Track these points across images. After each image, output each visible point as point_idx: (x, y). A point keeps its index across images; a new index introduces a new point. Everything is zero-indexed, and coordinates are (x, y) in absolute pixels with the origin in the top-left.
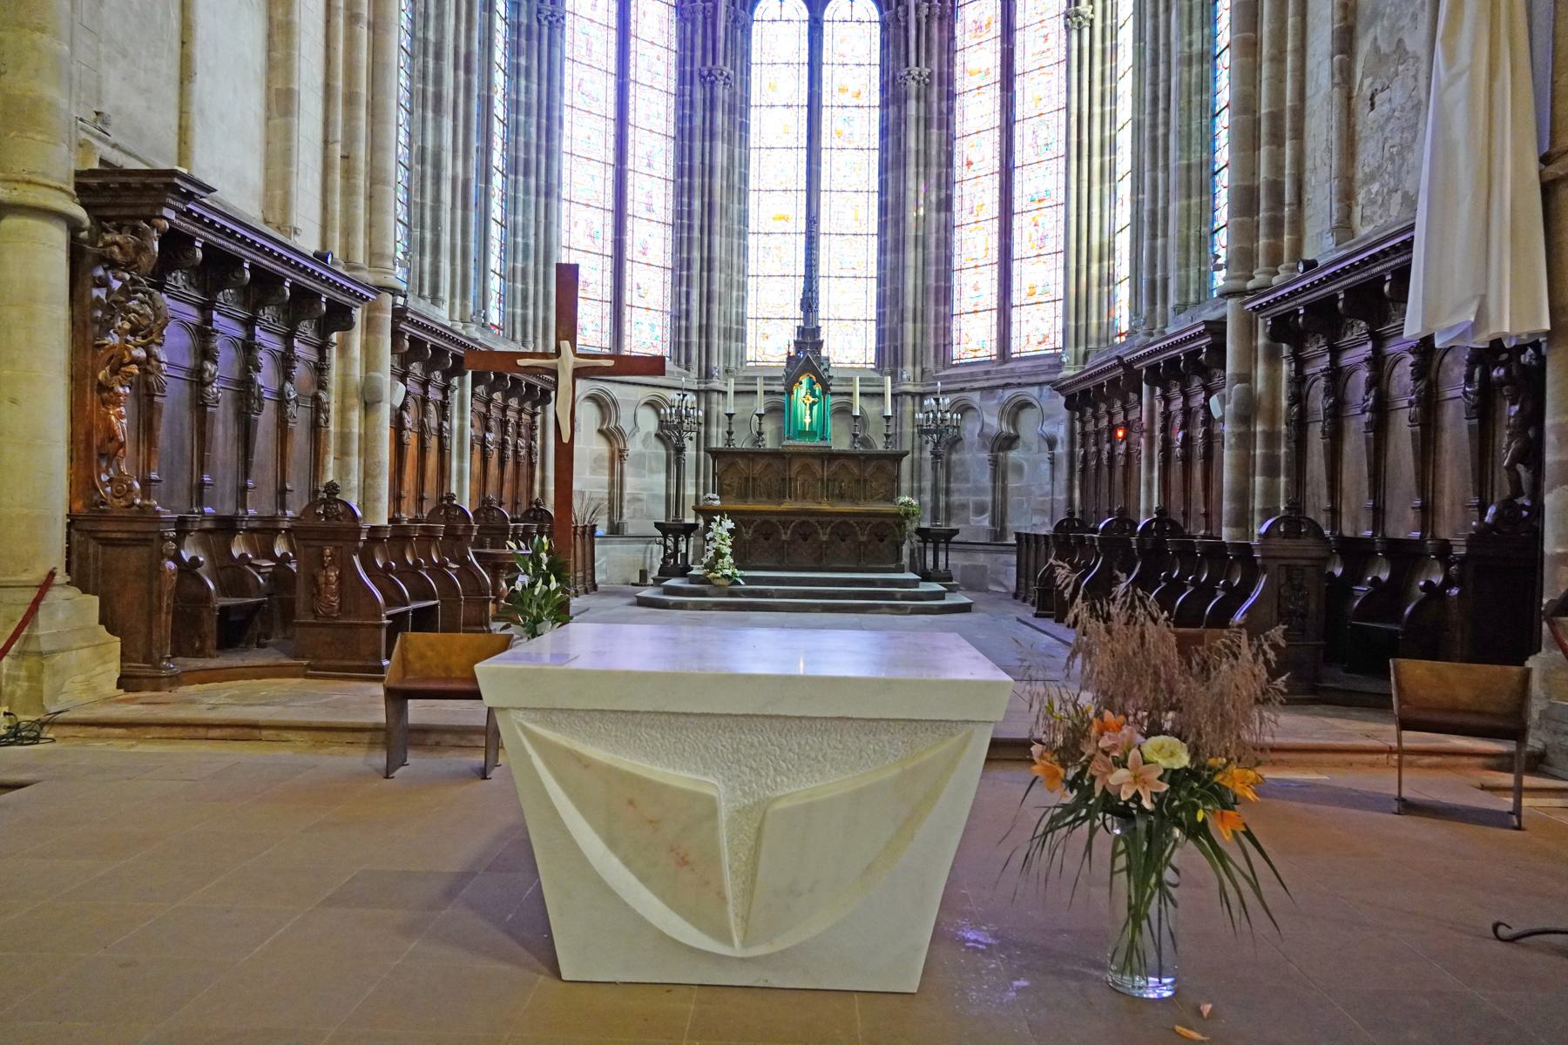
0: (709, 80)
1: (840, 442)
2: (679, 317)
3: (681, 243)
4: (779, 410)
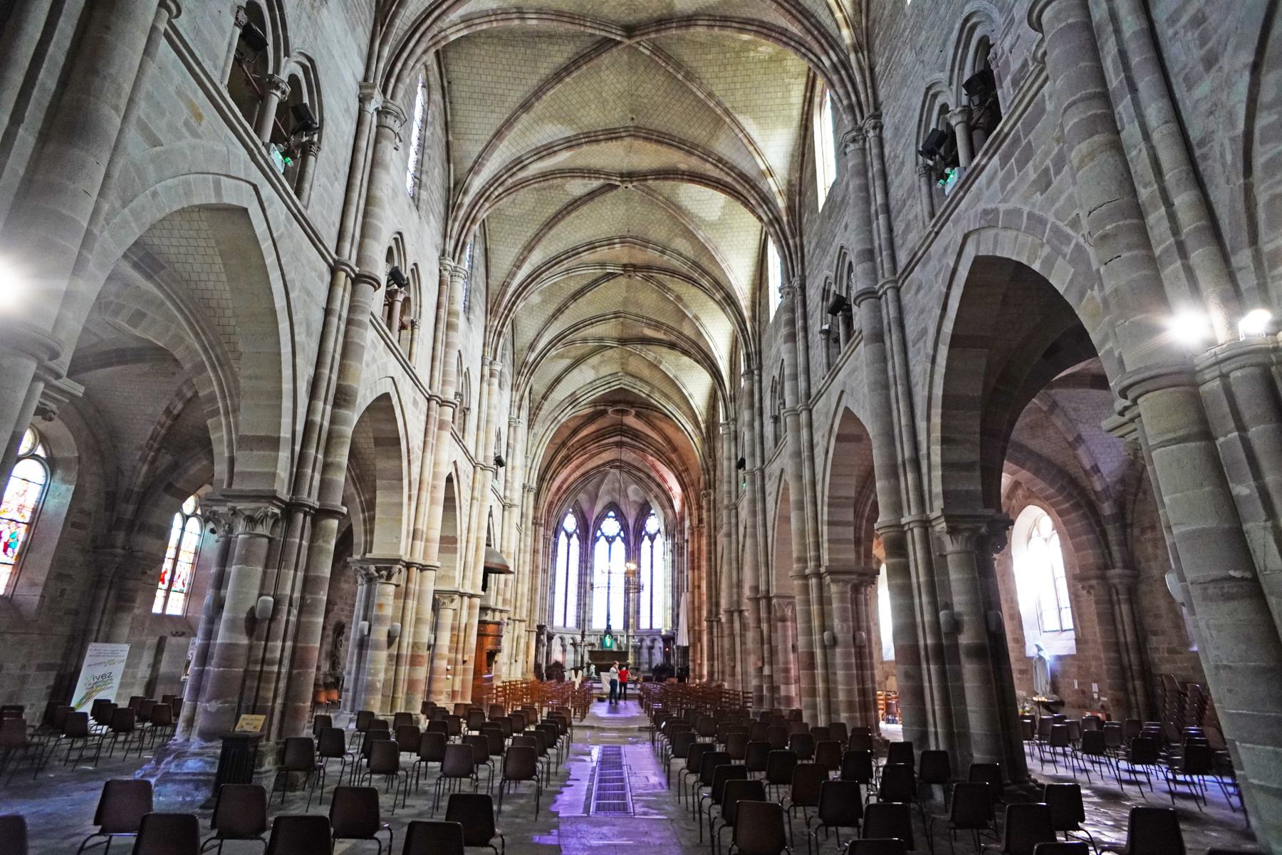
0: (586, 562)
1: (615, 649)
2: (578, 617)
3: (579, 599)
4: (602, 640)
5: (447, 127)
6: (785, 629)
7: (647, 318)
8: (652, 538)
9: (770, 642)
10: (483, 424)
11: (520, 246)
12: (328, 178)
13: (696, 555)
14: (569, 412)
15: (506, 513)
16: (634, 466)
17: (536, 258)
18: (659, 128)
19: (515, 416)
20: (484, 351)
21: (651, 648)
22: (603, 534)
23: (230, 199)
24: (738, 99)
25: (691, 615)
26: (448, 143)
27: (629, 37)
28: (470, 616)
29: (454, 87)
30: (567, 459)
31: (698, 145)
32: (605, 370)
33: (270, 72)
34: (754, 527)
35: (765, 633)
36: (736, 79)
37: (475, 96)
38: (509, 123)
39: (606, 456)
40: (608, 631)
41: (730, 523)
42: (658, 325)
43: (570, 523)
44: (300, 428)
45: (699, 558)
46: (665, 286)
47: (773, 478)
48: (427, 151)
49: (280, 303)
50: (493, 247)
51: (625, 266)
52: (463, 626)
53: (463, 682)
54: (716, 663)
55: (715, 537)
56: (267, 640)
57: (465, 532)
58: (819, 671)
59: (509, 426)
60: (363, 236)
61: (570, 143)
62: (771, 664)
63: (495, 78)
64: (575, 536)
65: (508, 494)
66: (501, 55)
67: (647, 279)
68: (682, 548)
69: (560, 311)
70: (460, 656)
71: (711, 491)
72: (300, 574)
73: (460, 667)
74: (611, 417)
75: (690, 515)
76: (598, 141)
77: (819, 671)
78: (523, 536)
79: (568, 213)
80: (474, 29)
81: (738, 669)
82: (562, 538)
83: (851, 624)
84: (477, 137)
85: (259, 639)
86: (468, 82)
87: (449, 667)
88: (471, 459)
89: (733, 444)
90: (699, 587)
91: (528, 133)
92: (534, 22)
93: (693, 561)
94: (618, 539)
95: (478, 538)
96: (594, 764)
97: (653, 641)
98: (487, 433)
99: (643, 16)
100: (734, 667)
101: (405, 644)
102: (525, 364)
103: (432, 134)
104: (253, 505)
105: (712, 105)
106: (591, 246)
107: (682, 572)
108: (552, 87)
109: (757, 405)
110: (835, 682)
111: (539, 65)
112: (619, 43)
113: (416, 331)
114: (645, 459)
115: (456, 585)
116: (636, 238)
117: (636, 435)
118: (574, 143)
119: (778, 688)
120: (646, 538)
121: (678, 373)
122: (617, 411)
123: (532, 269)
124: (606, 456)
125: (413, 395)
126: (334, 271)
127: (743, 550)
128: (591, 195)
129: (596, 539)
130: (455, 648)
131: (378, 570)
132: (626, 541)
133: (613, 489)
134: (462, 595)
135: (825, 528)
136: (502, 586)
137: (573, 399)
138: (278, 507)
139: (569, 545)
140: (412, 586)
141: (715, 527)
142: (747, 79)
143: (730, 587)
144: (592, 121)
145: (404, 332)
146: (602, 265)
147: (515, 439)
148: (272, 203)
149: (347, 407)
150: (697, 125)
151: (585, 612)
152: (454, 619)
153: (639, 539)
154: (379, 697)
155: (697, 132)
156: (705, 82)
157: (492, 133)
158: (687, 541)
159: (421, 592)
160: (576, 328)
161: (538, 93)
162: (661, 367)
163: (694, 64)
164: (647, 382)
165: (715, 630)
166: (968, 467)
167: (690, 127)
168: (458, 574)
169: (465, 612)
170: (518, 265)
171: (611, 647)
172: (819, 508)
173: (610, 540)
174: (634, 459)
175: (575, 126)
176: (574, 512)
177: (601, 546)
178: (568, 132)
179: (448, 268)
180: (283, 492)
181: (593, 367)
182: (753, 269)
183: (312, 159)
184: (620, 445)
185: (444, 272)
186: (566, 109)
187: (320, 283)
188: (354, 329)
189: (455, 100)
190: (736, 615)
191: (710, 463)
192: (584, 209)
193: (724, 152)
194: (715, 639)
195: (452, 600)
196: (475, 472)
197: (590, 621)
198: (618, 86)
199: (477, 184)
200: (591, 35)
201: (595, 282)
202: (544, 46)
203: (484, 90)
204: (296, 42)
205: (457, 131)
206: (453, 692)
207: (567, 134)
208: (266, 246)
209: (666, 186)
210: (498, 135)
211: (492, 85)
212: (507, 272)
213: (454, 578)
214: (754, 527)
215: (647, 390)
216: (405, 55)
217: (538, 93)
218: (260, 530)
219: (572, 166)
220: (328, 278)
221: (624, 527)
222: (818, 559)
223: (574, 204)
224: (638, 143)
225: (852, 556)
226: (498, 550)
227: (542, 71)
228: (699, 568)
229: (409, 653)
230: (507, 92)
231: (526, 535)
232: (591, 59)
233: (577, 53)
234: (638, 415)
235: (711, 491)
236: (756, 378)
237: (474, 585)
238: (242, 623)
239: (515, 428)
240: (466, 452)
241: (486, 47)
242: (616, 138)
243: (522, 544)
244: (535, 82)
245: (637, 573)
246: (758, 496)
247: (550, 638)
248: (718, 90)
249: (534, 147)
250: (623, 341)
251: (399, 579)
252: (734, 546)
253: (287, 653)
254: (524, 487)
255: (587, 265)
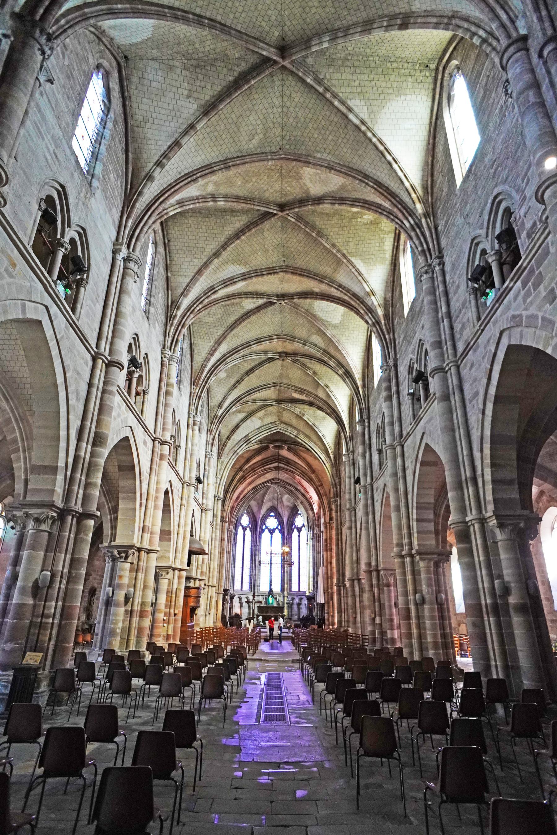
0: (256, 546)
1: (275, 605)
2: (250, 583)
3: (251, 572)
5: (167, 268)
6: (389, 592)
7: (295, 386)
8: (299, 530)
9: (379, 600)
10: (188, 456)
11: (212, 341)
12: (92, 301)
13: (328, 542)
14: (244, 448)
15: (203, 514)
16: (287, 483)
17: (223, 349)
18: (301, 267)
19: (209, 451)
20: (189, 409)
21: (299, 604)
22: (267, 528)
23: (30, 315)
24: (351, 247)
25: (325, 582)
26: (167, 278)
27: (282, 211)
28: (179, 583)
29: (172, 243)
30: (243, 478)
31: (326, 277)
32: (268, 420)
33: (58, 237)
34: (367, 523)
35: (376, 594)
36: (349, 235)
37: (185, 248)
38: (206, 265)
39: (269, 476)
40: (271, 593)
41: (351, 520)
42: (301, 391)
43: (245, 520)
44: (71, 460)
45: (330, 544)
46: (305, 366)
47: (379, 490)
48: (155, 283)
49: (60, 379)
50: (195, 342)
51: (280, 353)
52: (174, 590)
53: (174, 628)
54: (343, 614)
55: (341, 530)
56: (45, 602)
57: (176, 527)
58: (413, 621)
59: (206, 457)
60: (113, 336)
61: (245, 277)
62: (381, 616)
63: (198, 237)
64: (248, 529)
65: (204, 501)
66: (201, 223)
67: (294, 361)
68: (319, 537)
69: (238, 382)
70: (172, 611)
71: (338, 499)
72: (69, 556)
73: (172, 618)
74: (272, 450)
75: (324, 514)
76: (262, 275)
77: (413, 621)
78: (214, 529)
79: (244, 320)
80: (185, 208)
81: (358, 619)
82: (240, 530)
83: (434, 588)
84: (185, 274)
85: (40, 600)
86: (181, 240)
87: (165, 618)
88: (180, 479)
89: (352, 467)
90: (331, 563)
91: (218, 271)
92: (222, 203)
93: (326, 545)
94: (277, 531)
95: (185, 531)
96: (262, 686)
97: (301, 599)
98: (191, 461)
99: (290, 198)
100: (356, 618)
101: (136, 603)
102: (215, 416)
103: (158, 272)
104: (39, 511)
105: (335, 252)
106: (258, 341)
107: (319, 553)
108: (233, 242)
109: (367, 442)
110: (425, 629)
111: (225, 229)
112: (276, 214)
113: (146, 396)
114: (294, 478)
115: (170, 563)
116: (287, 335)
117: (288, 462)
118: (247, 276)
119: (386, 632)
120: (295, 530)
121: (315, 422)
122: (276, 447)
123: (220, 356)
124: (269, 476)
125: (143, 437)
126: (94, 359)
127: (360, 538)
128: (259, 309)
129: (263, 531)
130: (169, 605)
131: (119, 553)
132: (282, 532)
133: (273, 498)
134: (174, 569)
135: (415, 523)
136: (200, 563)
137: (247, 439)
138: (55, 512)
139: (244, 535)
140: (141, 563)
141: (341, 523)
142: (356, 235)
143: (352, 563)
144: (259, 263)
145: (138, 397)
146: (266, 353)
147: (209, 466)
148: (56, 317)
149: (100, 446)
150: (325, 264)
151: (255, 580)
152: (169, 586)
153: (291, 531)
154: (118, 639)
155: (325, 269)
156: (330, 237)
157: (195, 271)
158: (323, 532)
159: (147, 567)
160: (248, 393)
161: (224, 246)
162: (304, 418)
163: (323, 227)
164: (295, 428)
165: (342, 592)
166: (510, 482)
167: (321, 265)
168: (171, 555)
169: (176, 581)
170: (212, 353)
171: (272, 603)
172: (410, 510)
173: (272, 532)
174: (287, 478)
175: (247, 266)
176: (248, 513)
177: (266, 535)
178: (244, 270)
179: (167, 356)
180: (59, 503)
181: (260, 418)
182: (363, 354)
183: (82, 289)
184: (277, 468)
185: (164, 359)
186: (242, 255)
187: (85, 367)
188: (107, 396)
189: (172, 251)
190: (356, 582)
191: (337, 481)
192: (254, 318)
193: (343, 280)
194: (342, 598)
195: (168, 573)
196: (183, 488)
197: (259, 586)
198: (275, 241)
199: (185, 303)
200: (258, 210)
201: (261, 364)
202: (228, 217)
203: (190, 245)
204: (75, 219)
205: (173, 270)
206: (168, 635)
207: (243, 271)
208: (52, 344)
209: (304, 303)
210: (199, 272)
211: (196, 242)
212: (204, 358)
213: (169, 558)
214: (367, 523)
215: (295, 432)
216: (141, 225)
217: (224, 246)
218: (43, 527)
219: (246, 290)
220: (90, 363)
221: (281, 523)
222: (410, 544)
223: (248, 314)
224: (288, 276)
225: (433, 542)
226: (198, 539)
227: (227, 233)
228: (331, 550)
229: (139, 609)
230: (205, 246)
231: (216, 529)
232: (258, 225)
233: (249, 221)
234: (289, 449)
235: (338, 499)
236: (366, 424)
237: (182, 562)
238: (30, 590)
239: (209, 458)
240: (177, 474)
241: (192, 218)
242: (274, 273)
243: (214, 535)
244: (222, 239)
245: (290, 554)
246: (370, 502)
247: (232, 598)
248: (338, 242)
249: (221, 279)
250: (279, 401)
251: (133, 559)
252: (354, 535)
253: (59, 610)
254: (215, 497)
255: (256, 353)
